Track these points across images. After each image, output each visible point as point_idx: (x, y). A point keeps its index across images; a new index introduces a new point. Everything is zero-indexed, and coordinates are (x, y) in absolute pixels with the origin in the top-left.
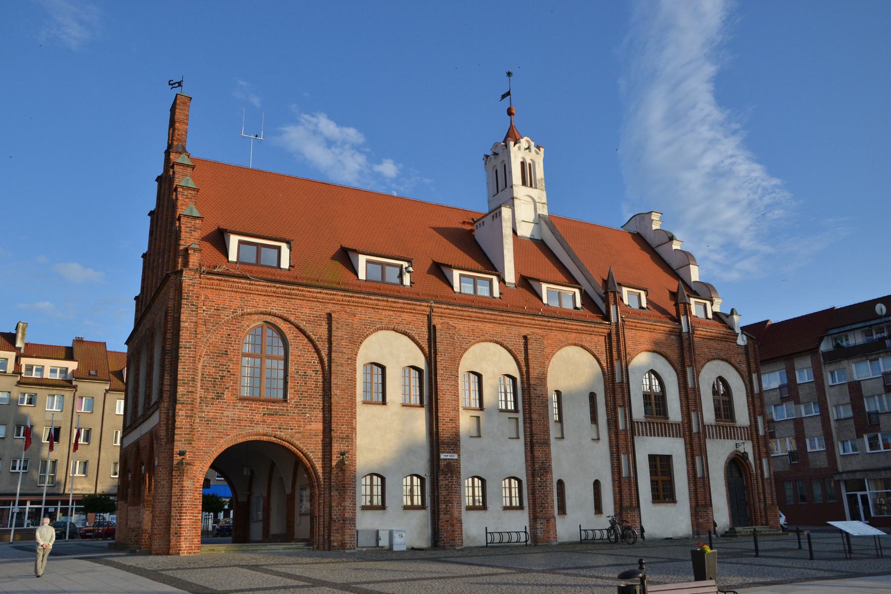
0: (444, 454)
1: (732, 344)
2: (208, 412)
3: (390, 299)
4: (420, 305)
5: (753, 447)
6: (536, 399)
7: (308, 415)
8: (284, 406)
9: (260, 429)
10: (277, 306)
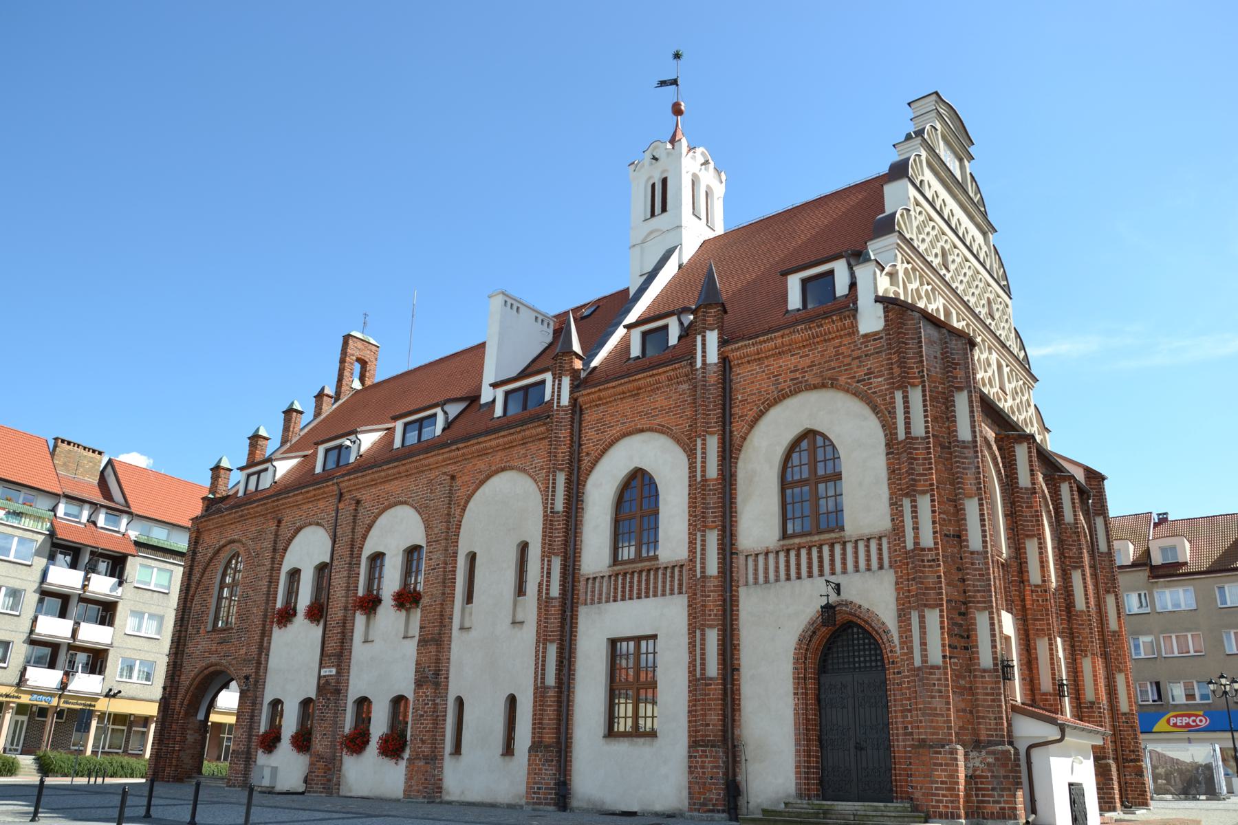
1: (846, 341)
4: (328, 486)
5: (897, 583)
6: (429, 574)
9: (214, 659)
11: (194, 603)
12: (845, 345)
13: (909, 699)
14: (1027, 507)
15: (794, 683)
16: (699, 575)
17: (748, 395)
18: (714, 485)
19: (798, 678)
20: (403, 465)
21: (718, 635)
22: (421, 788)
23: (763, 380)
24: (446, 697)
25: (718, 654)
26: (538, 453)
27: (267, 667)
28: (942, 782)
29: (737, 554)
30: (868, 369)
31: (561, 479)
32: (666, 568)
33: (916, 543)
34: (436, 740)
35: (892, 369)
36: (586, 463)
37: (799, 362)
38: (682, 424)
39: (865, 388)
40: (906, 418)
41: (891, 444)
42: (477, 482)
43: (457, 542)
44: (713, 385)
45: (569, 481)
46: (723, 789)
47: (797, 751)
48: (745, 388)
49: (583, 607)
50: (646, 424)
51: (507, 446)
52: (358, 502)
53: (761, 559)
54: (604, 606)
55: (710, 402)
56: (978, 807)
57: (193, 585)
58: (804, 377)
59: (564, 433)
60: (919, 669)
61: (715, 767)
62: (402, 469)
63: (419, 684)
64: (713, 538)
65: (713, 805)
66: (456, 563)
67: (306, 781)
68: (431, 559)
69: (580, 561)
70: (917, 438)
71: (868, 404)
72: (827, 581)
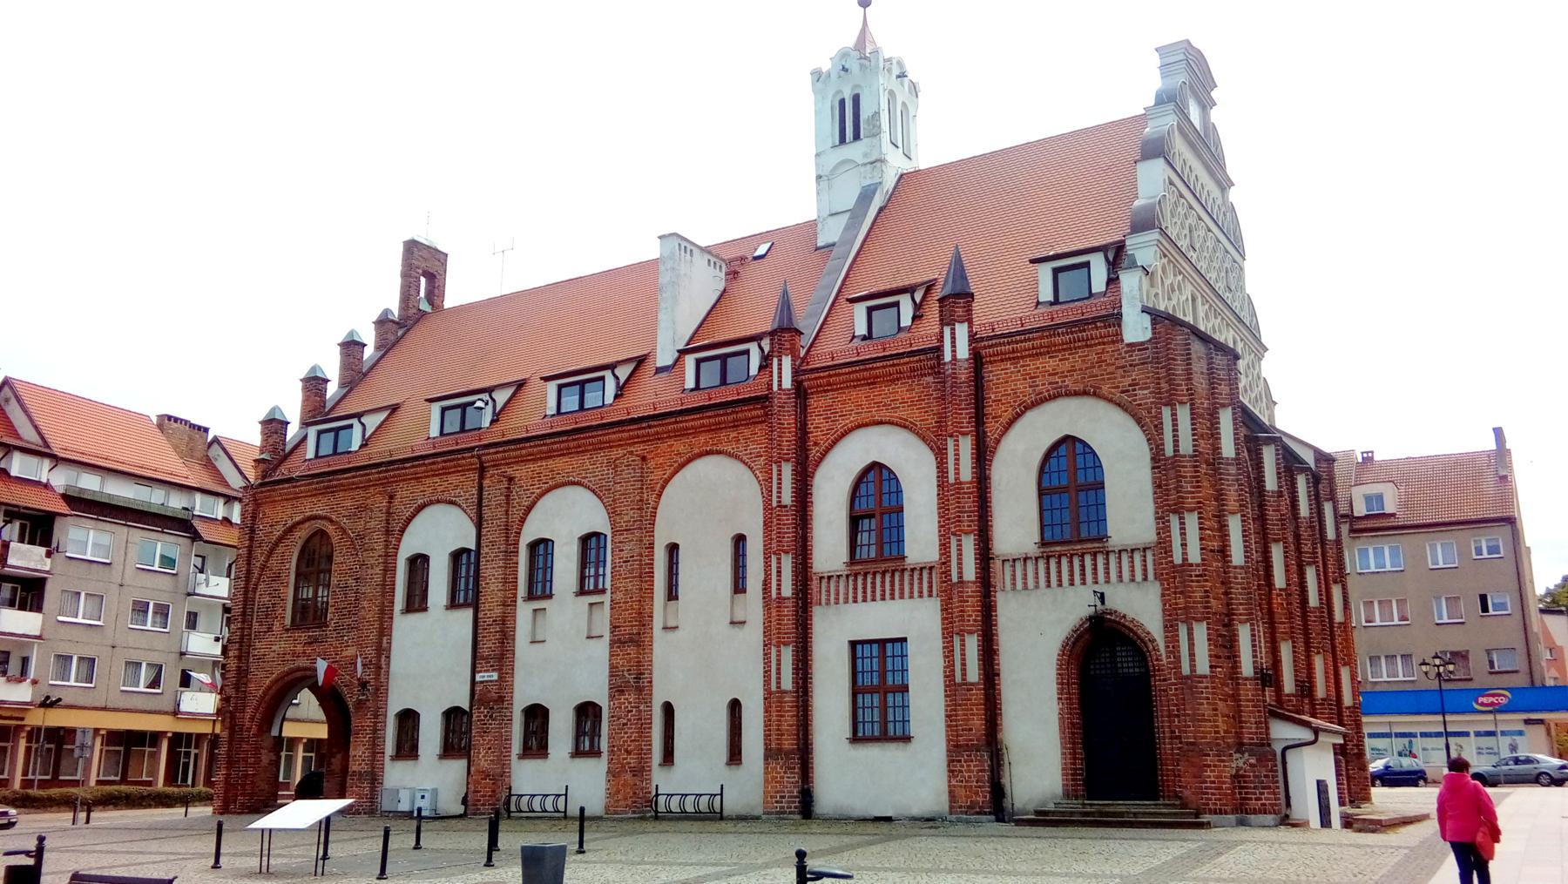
0: (480, 674)
1: (1109, 348)
2: (260, 649)
3: (426, 462)
4: (464, 458)
5: (1163, 595)
6: (621, 567)
7: (346, 638)
8: (323, 631)
10: (319, 507)
11: (258, 593)
12: (1108, 352)
13: (1176, 705)
14: (1273, 511)
15: (1058, 689)
16: (955, 579)
17: (1002, 396)
18: (968, 488)
19: (1062, 684)
20: (574, 440)
21: (978, 640)
22: (630, 803)
23: (1019, 380)
24: (650, 702)
25: (979, 660)
26: (755, 440)
27: (388, 672)
28: (1214, 782)
29: (993, 558)
30: (1133, 380)
31: (787, 470)
32: (913, 570)
33: (1185, 559)
34: (642, 750)
35: (1159, 384)
36: (814, 452)
37: (1058, 365)
38: (928, 420)
39: (1130, 399)
40: (1174, 436)
41: (1157, 458)
42: (676, 465)
43: (653, 532)
44: (963, 383)
45: (796, 473)
46: (990, 792)
47: (1063, 754)
48: (999, 388)
49: (818, 607)
50: (886, 416)
51: (713, 428)
52: (511, 479)
53: (1019, 566)
54: (842, 605)
55: (962, 400)
56: (1241, 804)
57: (256, 572)
58: (1065, 381)
59: (789, 420)
60: (1187, 677)
61: (981, 771)
62: (572, 444)
63: (616, 690)
64: (969, 545)
65: (980, 807)
66: (653, 555)
67: (465, 801)
68: (623, 550)
69: (811, 559)
70: (1185, 456)
71: (1133, 416)
72: (1095, 592)
